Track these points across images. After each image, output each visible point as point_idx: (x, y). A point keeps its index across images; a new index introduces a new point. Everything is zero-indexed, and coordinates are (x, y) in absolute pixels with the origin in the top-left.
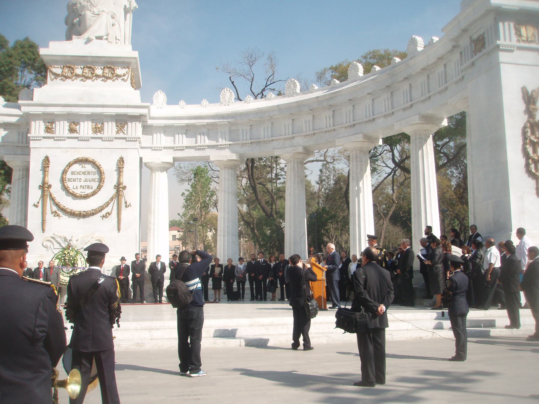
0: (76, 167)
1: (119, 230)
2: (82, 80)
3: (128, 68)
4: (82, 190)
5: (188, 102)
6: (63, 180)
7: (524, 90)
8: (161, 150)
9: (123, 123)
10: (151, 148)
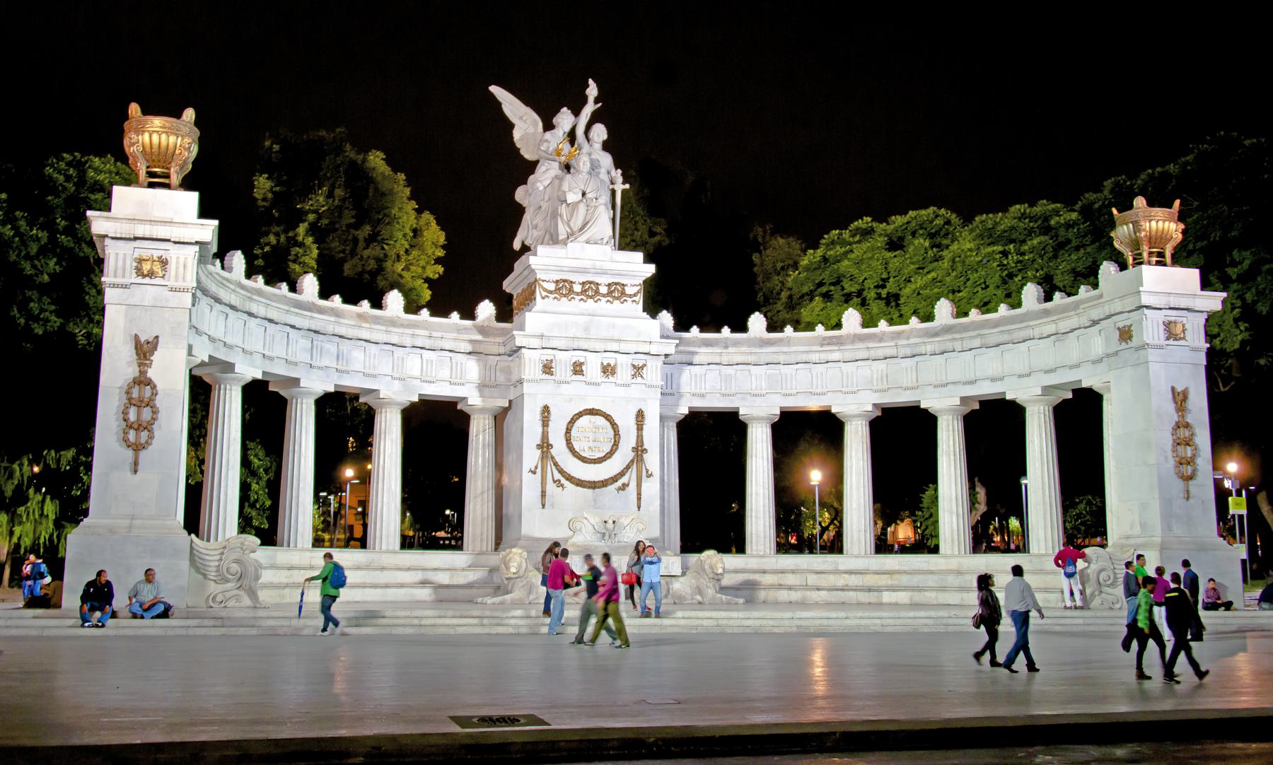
1: (639, 508)
7: (1173, 389)
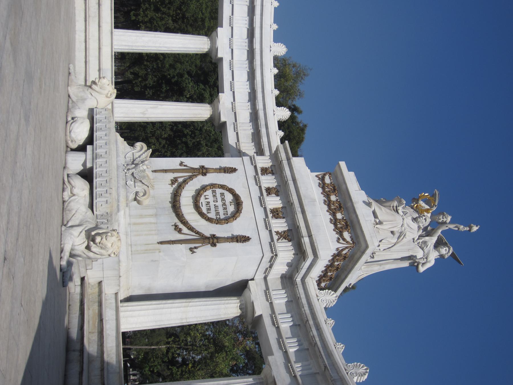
0: (229, 197)
1: (161, 243)
2: (325, 201)
3: (353, 242)
4: (204, 204)
5: (334, 329)
6: (213, 186)
8: (267, 300)
9: (290, 237)
10: (267, 288)
